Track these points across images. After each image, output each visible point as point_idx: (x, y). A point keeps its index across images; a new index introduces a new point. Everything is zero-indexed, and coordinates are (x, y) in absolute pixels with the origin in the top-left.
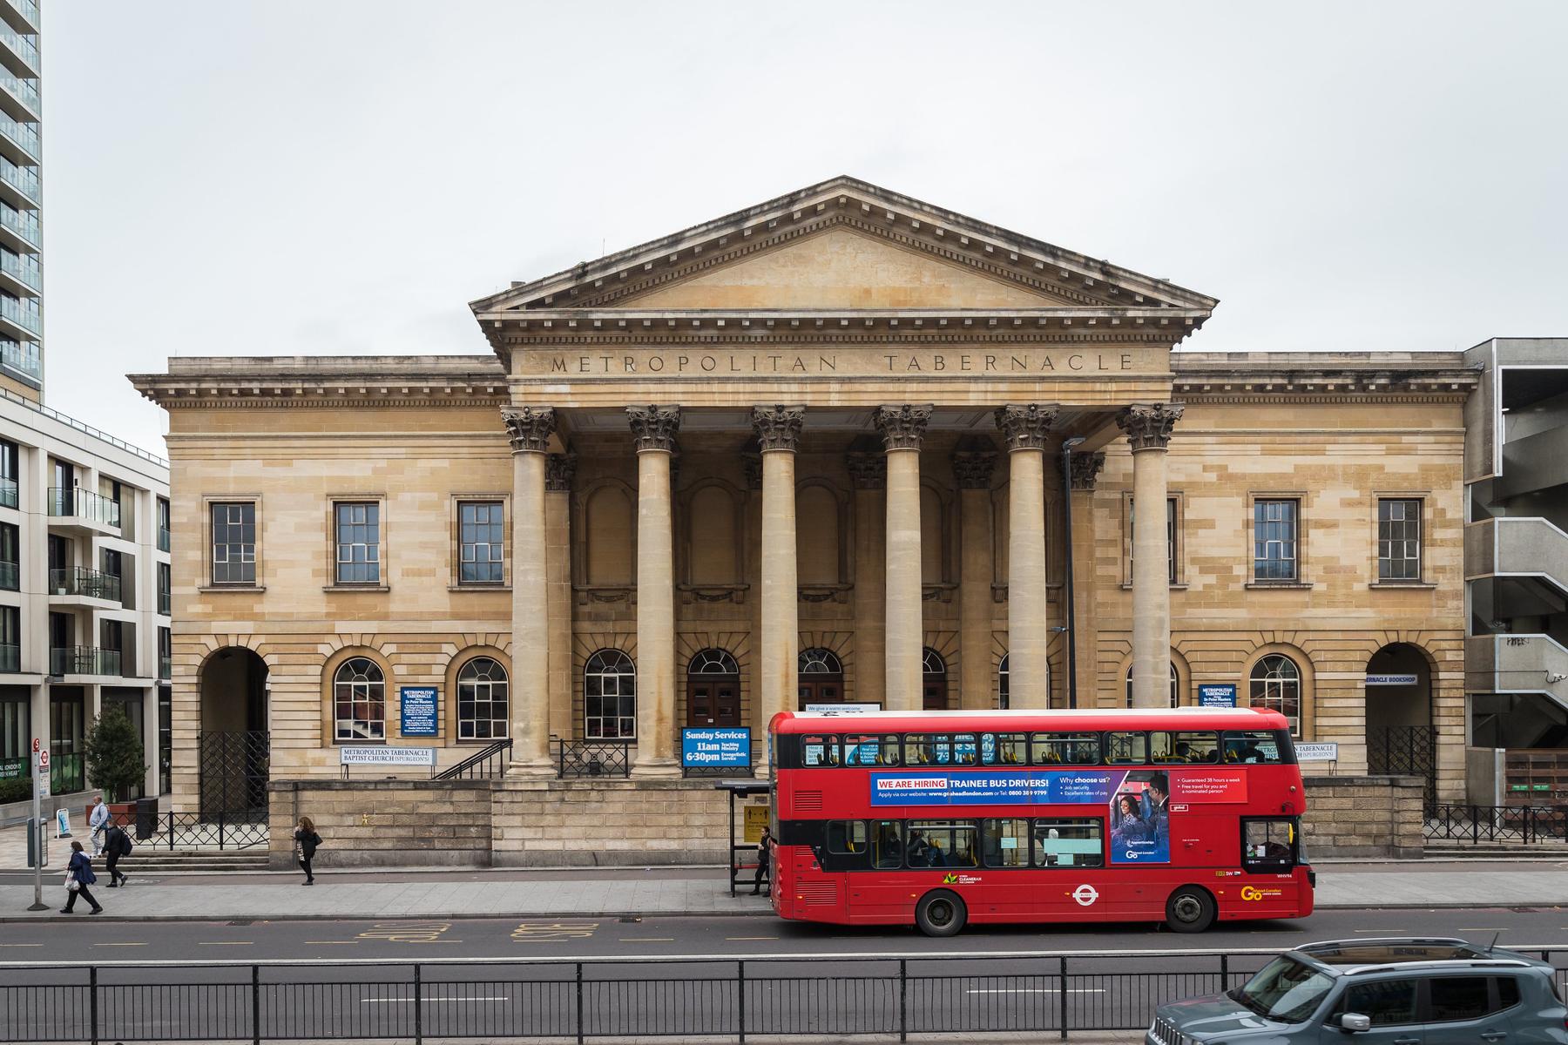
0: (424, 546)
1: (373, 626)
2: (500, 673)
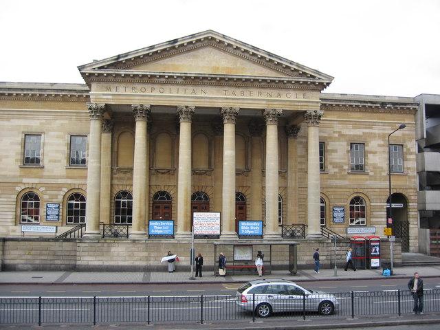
0: (57, 151)
1: (37, 181)
2: (83, 199)
